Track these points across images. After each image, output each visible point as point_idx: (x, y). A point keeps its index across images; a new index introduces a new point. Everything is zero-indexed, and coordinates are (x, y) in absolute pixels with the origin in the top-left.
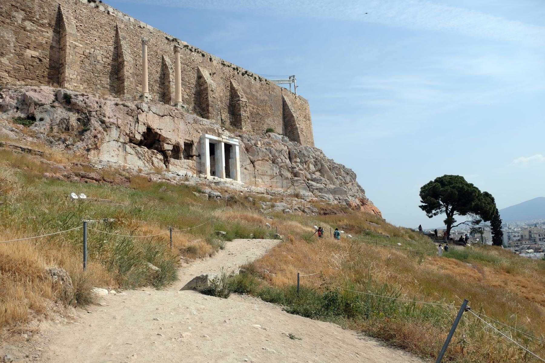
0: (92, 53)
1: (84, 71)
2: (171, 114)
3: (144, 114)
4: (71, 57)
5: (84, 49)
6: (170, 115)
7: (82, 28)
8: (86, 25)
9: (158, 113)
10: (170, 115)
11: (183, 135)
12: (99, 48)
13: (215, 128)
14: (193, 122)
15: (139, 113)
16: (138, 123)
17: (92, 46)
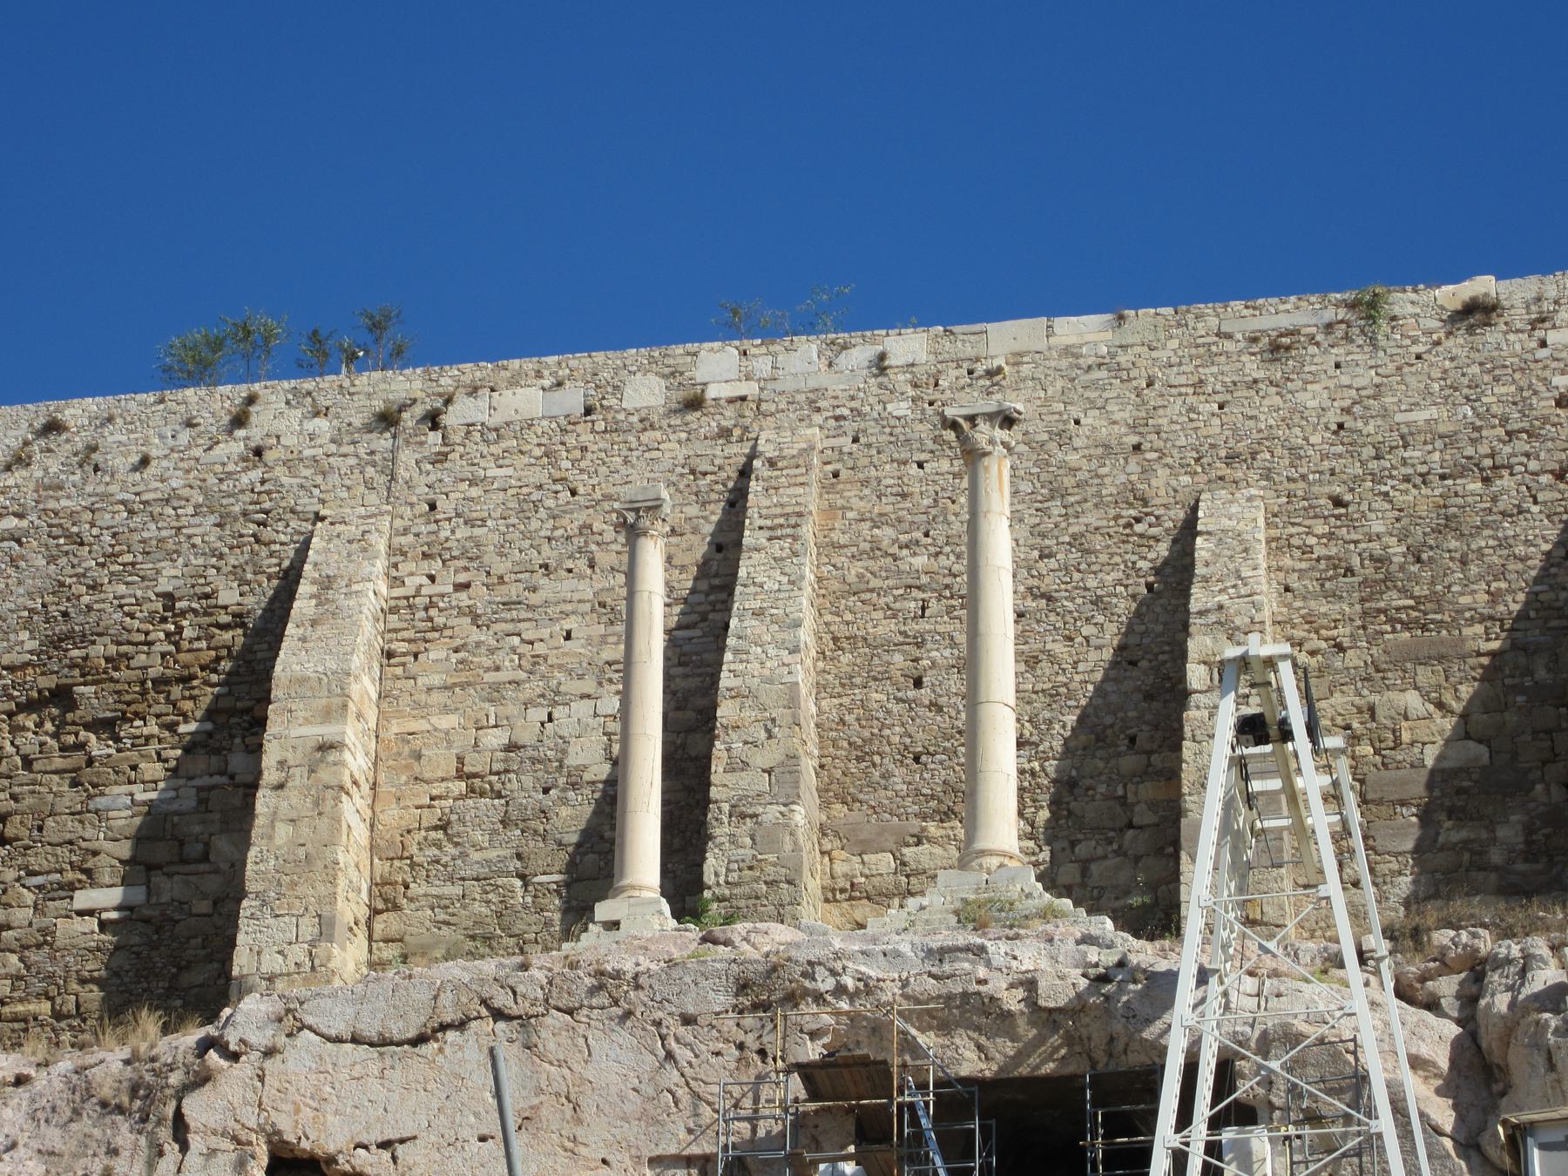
0: (526, 736)
1: (457, 890)
2: (502, 1000)
3: (245, 1069)
4: (283, 832)
5: (462, 742)
6: (498, 1015)
7: (479, 597)
8: (500, 567)
9: (370, 1030)
10: (498, 1015)
11: (632, 1131)
12: (588, 686)
13: (998, 986)
14: (722, 1000)
15: (201, 1079)
16: (185, 1148)
17: (533, 688)
